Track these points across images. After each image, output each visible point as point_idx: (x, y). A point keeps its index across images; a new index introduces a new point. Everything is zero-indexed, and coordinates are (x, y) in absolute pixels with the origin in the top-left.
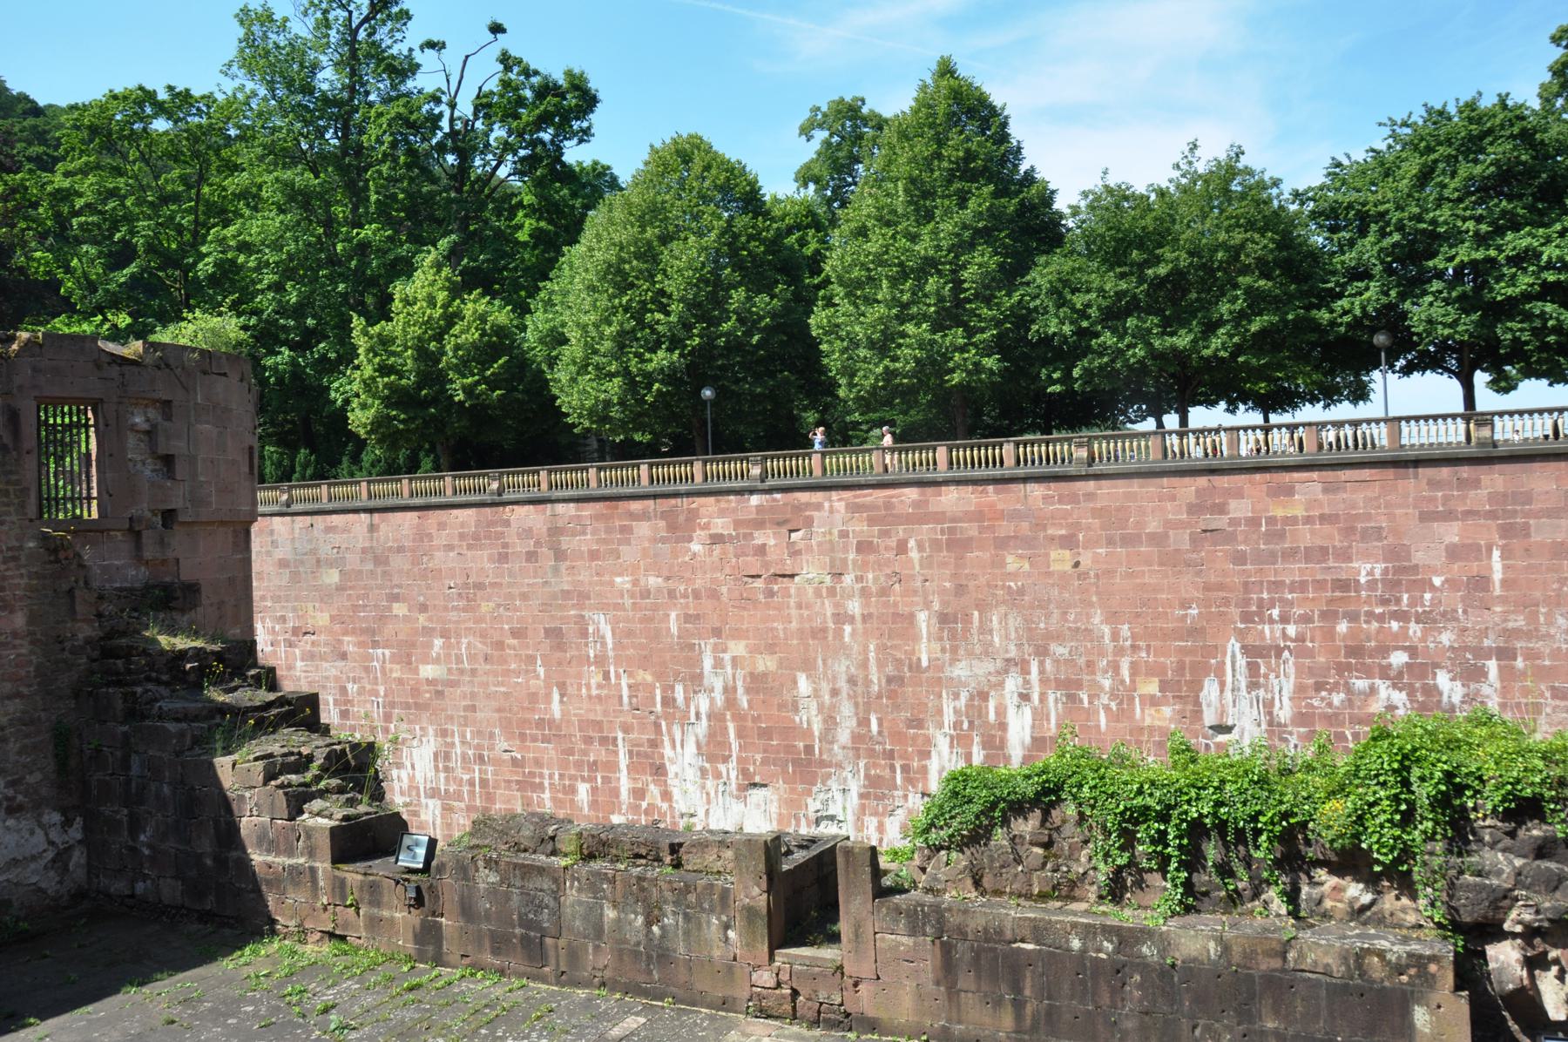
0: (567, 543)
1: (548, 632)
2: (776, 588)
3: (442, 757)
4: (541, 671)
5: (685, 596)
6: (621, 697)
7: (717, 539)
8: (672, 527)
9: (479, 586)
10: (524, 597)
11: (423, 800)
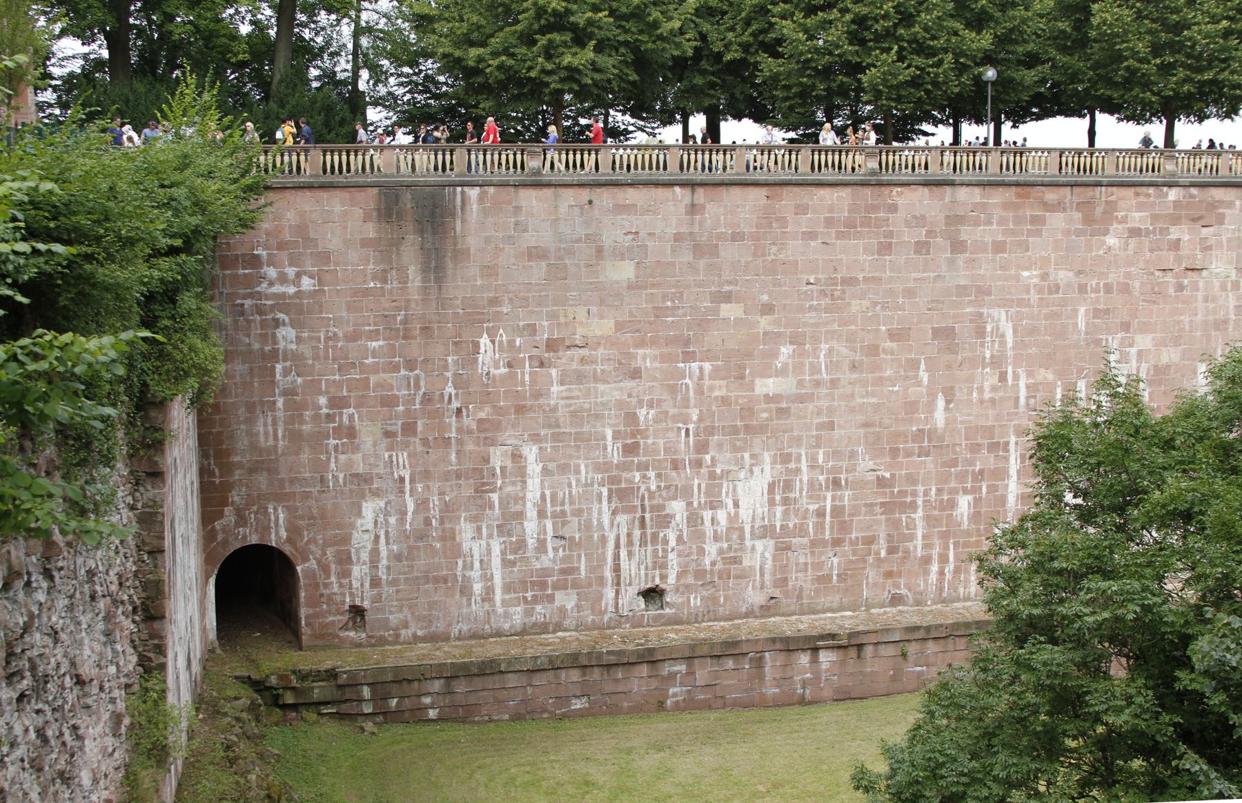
0: (966, 233)
1: (936, 333)
2: (1186, 282)
3: (781, 489)
4: (924, 376)
5: (1096, 291)
6: (1017, 398)
7: (1134, 232)
8: (1088, 220)
9: (849, 281)
10: (909, 293)
11: (748, 543)
